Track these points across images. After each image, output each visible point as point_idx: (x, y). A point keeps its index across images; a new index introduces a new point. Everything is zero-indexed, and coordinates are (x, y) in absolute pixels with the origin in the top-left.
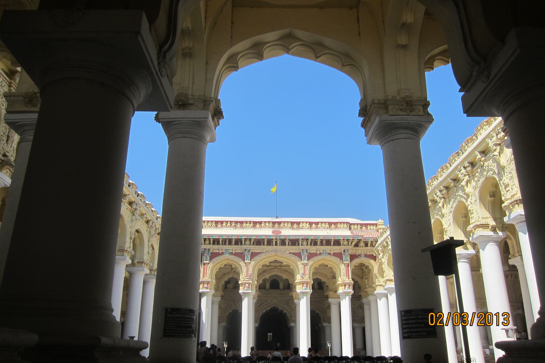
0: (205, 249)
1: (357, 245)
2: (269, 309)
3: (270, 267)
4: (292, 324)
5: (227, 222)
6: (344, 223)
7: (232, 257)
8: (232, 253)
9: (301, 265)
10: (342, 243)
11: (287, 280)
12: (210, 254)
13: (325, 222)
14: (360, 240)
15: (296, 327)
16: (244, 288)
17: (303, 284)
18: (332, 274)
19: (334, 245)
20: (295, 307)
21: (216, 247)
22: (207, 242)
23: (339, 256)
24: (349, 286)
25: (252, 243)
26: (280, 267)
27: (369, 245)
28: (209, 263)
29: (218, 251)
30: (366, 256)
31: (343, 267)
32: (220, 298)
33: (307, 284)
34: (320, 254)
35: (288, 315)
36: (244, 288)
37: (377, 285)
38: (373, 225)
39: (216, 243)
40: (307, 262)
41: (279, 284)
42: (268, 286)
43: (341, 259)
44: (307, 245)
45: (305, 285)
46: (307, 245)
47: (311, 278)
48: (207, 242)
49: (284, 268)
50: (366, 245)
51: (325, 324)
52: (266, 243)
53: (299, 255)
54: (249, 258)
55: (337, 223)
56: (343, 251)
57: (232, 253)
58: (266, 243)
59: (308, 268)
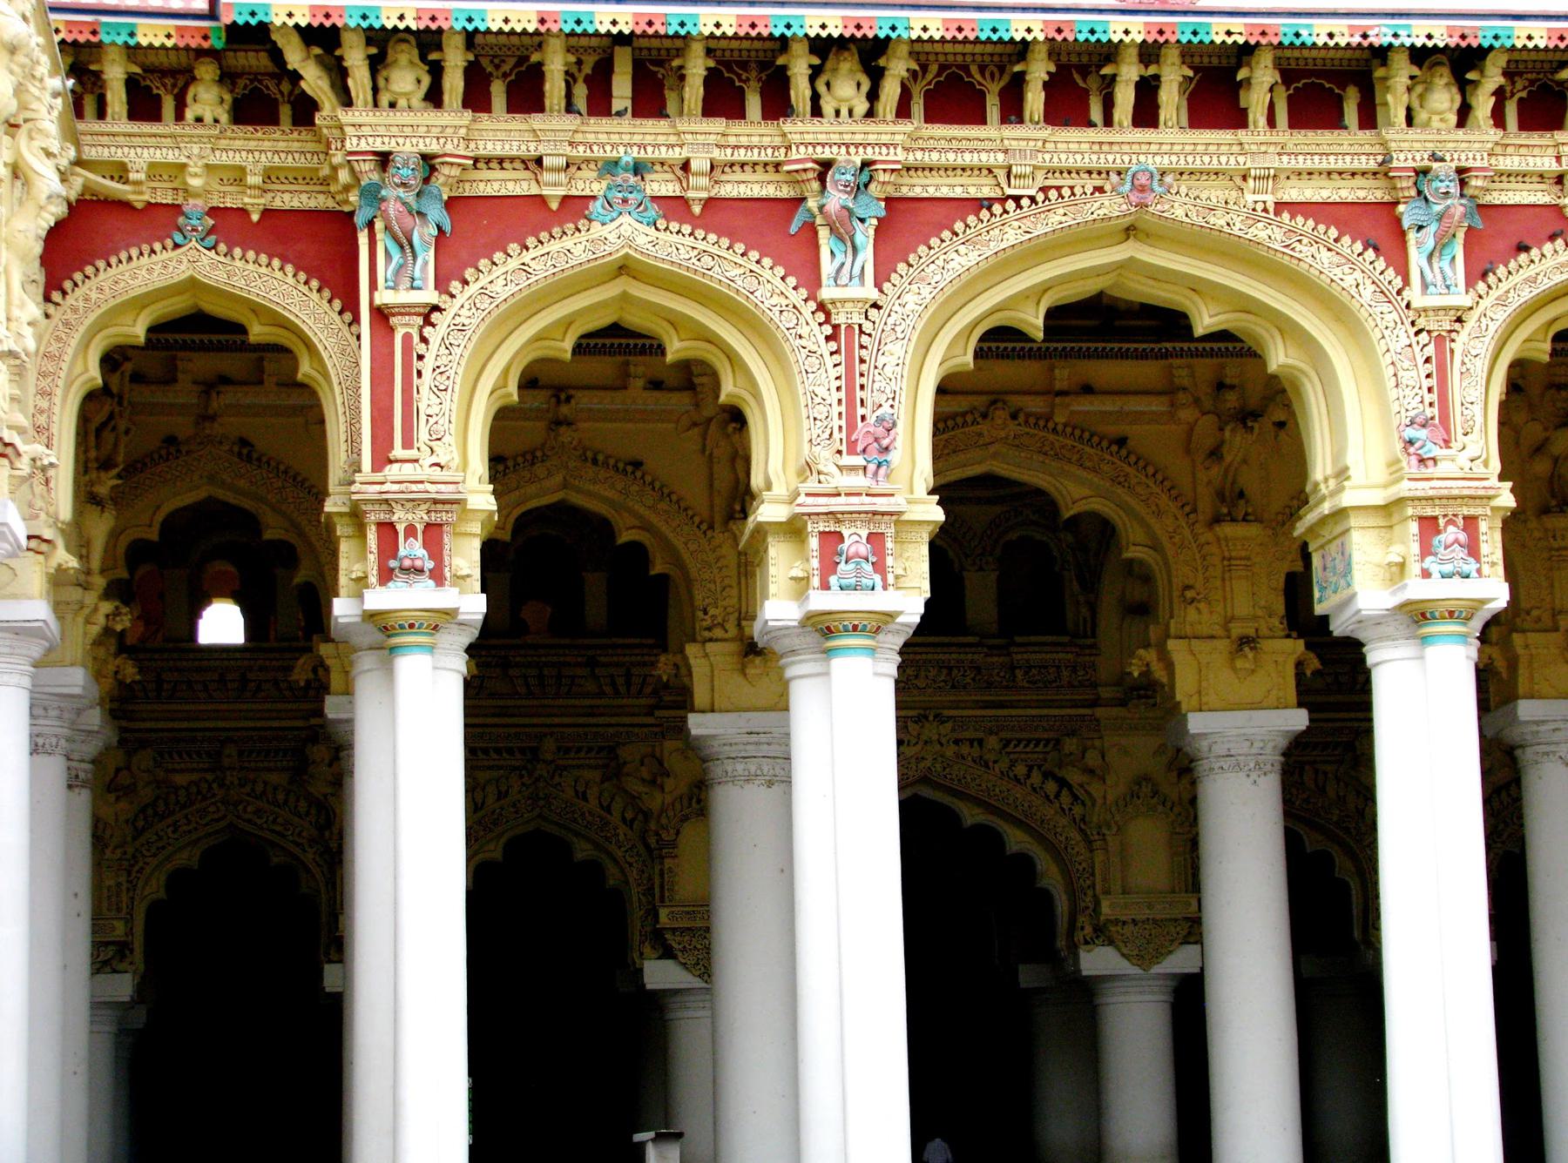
0: (384, 159)
9: (1404, 335)
12: (436, 213)
16: (829, 567)
17: (1429, 526)
21: (503, 132)
25: (891, 91)
26: (1035, 405)
29: (516, 184)
33: (1470, 523)
35: (1050, 875)
36: (829, 567)
39: (498, 92)
40: (1465, 300)
44: (1464, 115)
45: (1452, 533)
46: (1464, 115)
47: (1496, 465)
48: (406, 79)
49: (1085, 405)
52: (1035, 100)
53: (1380, 228)
54: (867, 255)
57: (674, 208)
58: (1035, 100)
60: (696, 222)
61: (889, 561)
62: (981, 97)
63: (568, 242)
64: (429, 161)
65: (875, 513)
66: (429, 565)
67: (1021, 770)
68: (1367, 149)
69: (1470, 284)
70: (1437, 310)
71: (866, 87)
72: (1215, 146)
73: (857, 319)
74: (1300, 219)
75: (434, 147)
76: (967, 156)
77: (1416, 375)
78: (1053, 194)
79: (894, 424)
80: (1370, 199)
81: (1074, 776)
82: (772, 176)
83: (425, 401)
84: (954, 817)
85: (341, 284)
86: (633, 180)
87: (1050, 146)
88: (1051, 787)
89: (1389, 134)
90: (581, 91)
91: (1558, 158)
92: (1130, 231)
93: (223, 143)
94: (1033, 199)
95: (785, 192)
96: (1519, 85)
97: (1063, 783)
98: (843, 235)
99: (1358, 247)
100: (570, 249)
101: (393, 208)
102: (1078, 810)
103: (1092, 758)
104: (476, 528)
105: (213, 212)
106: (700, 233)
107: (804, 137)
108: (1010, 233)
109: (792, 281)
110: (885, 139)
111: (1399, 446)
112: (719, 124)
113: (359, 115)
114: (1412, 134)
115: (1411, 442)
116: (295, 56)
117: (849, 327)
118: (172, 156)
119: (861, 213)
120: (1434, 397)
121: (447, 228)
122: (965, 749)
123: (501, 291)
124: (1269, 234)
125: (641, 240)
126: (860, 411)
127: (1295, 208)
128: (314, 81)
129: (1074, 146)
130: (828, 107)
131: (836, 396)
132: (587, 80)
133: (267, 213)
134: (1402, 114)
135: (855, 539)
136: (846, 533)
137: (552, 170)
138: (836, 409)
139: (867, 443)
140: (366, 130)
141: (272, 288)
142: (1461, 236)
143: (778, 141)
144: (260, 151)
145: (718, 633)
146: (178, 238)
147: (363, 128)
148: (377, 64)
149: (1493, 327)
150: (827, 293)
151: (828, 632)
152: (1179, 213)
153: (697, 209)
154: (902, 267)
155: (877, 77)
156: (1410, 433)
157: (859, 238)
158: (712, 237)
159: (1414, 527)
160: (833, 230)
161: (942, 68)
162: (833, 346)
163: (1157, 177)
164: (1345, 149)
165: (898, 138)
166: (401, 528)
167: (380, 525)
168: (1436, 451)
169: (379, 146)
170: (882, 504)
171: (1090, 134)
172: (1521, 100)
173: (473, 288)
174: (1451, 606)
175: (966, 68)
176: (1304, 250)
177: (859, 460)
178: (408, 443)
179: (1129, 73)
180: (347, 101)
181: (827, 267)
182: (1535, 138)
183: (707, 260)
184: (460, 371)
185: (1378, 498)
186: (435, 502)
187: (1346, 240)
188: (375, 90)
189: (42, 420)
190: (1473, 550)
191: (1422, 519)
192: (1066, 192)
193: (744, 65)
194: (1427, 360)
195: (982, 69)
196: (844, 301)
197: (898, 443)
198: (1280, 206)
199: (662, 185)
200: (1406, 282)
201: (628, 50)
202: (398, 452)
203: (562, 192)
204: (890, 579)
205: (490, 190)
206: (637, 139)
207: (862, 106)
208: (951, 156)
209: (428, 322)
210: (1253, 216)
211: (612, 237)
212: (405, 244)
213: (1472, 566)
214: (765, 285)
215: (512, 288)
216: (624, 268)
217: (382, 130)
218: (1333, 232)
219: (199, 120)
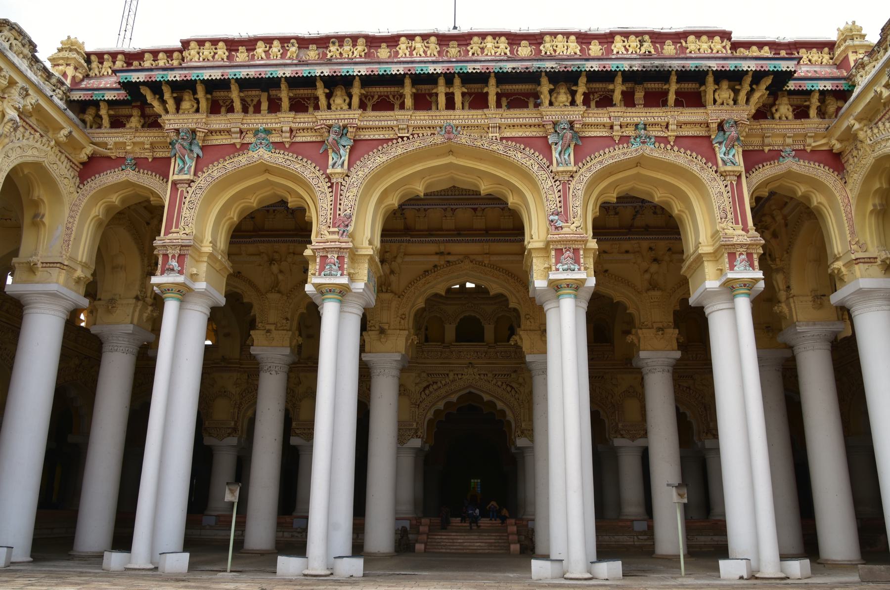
0: (177, 131)
1: (762, 114)
2: (454, 398)
3: (450, 258)
4: (521, 442)
5: (269, 41)
6: (711, 34)
7: (278, 159)
8: (279, 145)
9: (550, 182)
10: (709, 97)
11: (501, 299)
12: (197, 150)
13: (638, 34)
14: (789, 75)
15: (532, 448)
16: (322, 268)
17: (559, 252)
18: (647, 276)
19: (678, 104)
20: (531, 393)
21: (218, 122)
22: (186, 105)
23: (702, 145)
24: (750, 256)
27: (813, 112)
28: (190, 182)
30: (800, 154)
31: (717, 188)
32: (287, 351)
33: (576, 251)
34: (625, 139)
35: (510, 416)
36: (322, 268)
37: (857, 261)
38: (819, 46)
40: (572, 168)
41: (482, 330)
42: (450, 332)
43: (711, 157)
44: (573, 103)
49: (494, 258)
50: (801, 113)
51: (618, 442)
52: (409, 102)
55: (684, 35)
56: (714, 126)
57: (279, 145)
59: (578, 187)
60: (285, 149)
61: (346, 266)
62: (393, 105)
63: (240, 158)
64: (194, 132)
65: (340, 248)
66: (177, 268)
67: (499, 383)
68: (534, 115)
69: (576, 163)
70: (563, 172)
71: (347, 101)
72: (475, 117)
73: (340, 180)
74: (510, 143)
75: (194, 126)
76: (383, 123)
77: (554, 197)
78: (416, 136)
79: (350, 217)
80: (538, 135)
81: (514, 385)
82: (314, 134)
83: (185, 212)
84: (482, 398)
85: (165, 176)
86: (263, 136)
87: (413, 118)
88: (509, 389)
89: (541, 109)
90: (251, 109)
91: (610, 118)
92: (451, 152)
93: (137, 134)
94: (408, 138)
95: (319, 139)
96: (596, 96)
97: (512, 388)
98: (337, 152)
99: (532, 151)
100: (242, 160)
101: (177, 146)
102: (517, 396)
103: (521, 380)
104: (205, 259)
105: (135, 159)
106: (286, 153)
107: (323, 116)
108: (398, 150)
109: (318, 168)
110: (351, 116)
111: (548, 223)
112: (292, 114)
113: (169, 117)
114: (551, 108)
115: (552, 221)
116: (150, 97)
117: (337, 183)
118: (121, 140)
119: (344, 144)
120: (562, 204)
121: (201, 154)
122: (482, 377)
123: (216, 174)
124: (499, 148)
125: (266, 156)
126: (338, 212)
127: (507, 139)
128: (157, 107)
129: (422, 118)
130: (333, 107)
131: (330, 207)
132: (255, 106)
133: (154, 159)
134: (547, 102)
135: (333, 257)
136: (329, 256)
137: (235, 133)
138: (329, 212)
139: (341, 223)
140: (172, 121)
141: (148, 181)
142: (572, 146)
143: (314, 119)
144: (148, 137)
145: (373, 328)
146: (123, 167)
147: (171, 121)
148: (178, 102)
149: (585, 179)
150: (329, 171)
151: (322, 293)
152: (464, 141)
153: (287, 146)
154: (358, 163)
155: (350, 96)
156: (552, 217)
157: (342, 151)
158: (291, 154)
159: (553, 253)
160: (333, 151)
161: (379, 97)
162: (330, 190)
163: (455, 129)
164: (526, 115)
165: (356, 116)
166: (170, 256)
167: (164, 255)
168: (562, 224)
169: (176, 127)
170: (344, 245)
171: (430, 113)
172: (597, 102)
173: (205, 175)
174: (568, 282)
175: (388, 96)
176: (511, 153)
177: (336, 230)
178: (177, 227)
179: (441, 89)
180: (167, 112)
181: (331, 162)
182: (600, 111)
183: (288, 162)
184: (199, 203)
185: (541, 245)
186: (182, 246)
187: (527, 149)
188: (178, 109)
189: (70, 225)
190: (577, 261)
191: (556, 250)
192: (421, 135)
193: (309, 99)
194: (559, 191)
195: (394, 97)
196: (335, 174)
197: (353, 223)
198: (502, 139)
199: (275, 138)
200: (551, 163)
201: (266, 94)
202: (174, 230)
203: (239, 141)
204: (345, 272)
205: (217, 143)
206: (265, 121)
207: (346, 107)
208: (377, 123)
209: (190, 186)
210: (491, 142)
211: (256, 156)
212: (184, 162)
213: (577, 267)
214: (308, 171)
215: (220, 174)
216: (267, 169)
217: (177, 121)
218: (522, 146)
219: (131, 128)
